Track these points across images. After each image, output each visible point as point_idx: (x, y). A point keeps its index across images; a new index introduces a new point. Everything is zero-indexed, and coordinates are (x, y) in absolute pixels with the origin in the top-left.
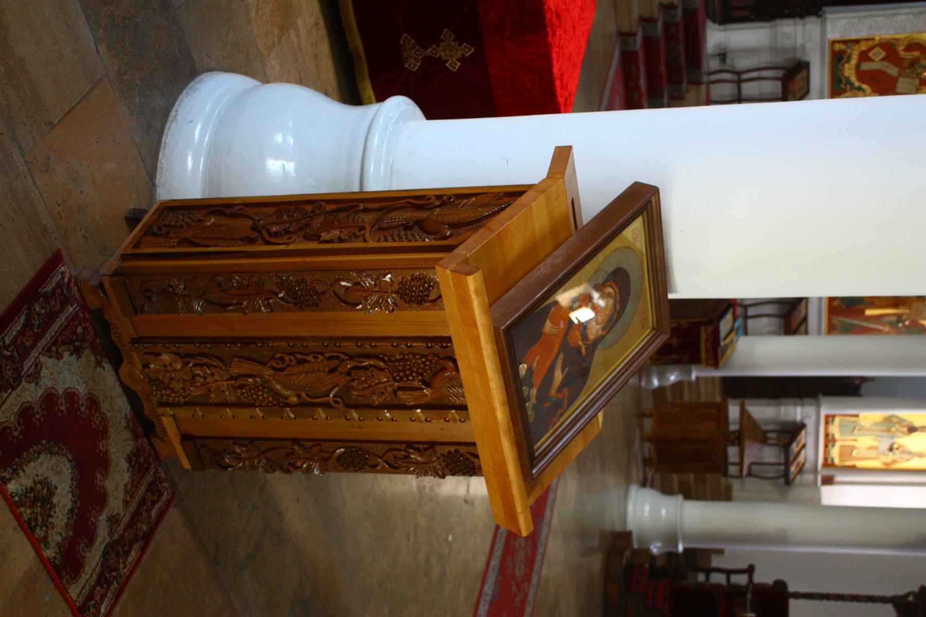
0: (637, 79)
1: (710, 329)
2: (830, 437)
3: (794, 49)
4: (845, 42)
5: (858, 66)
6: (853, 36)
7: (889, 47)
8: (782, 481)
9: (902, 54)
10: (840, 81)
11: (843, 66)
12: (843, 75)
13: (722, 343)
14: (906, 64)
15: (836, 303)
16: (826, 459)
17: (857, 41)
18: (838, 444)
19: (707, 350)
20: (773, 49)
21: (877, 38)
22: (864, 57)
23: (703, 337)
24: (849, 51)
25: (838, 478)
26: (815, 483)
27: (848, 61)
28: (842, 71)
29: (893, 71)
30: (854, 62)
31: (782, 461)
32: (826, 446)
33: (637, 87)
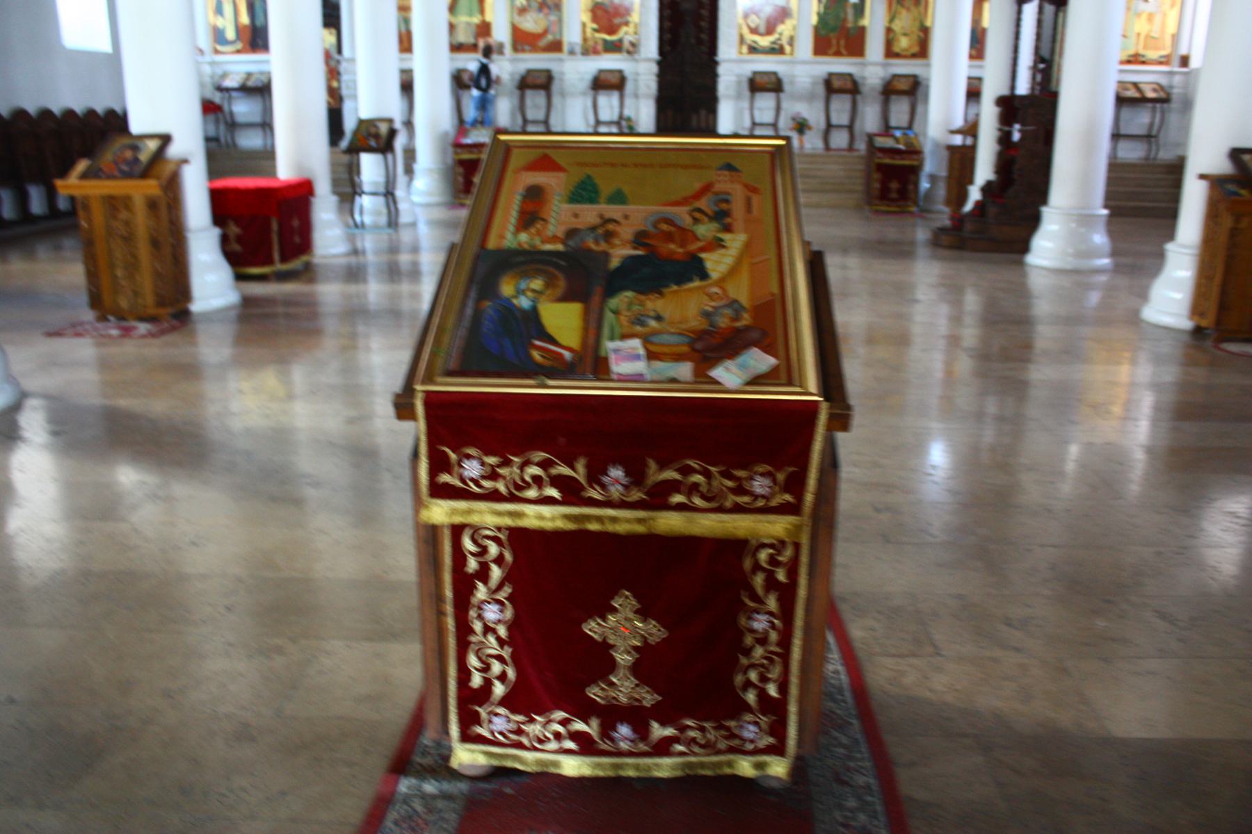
1: (880, 155)
2: (1131, 59)
3: (739, 83)
6: (736, 39)
8: (1165, 105)
11: (761, 47)
13: (901, 147)
15: (974, 53)
16: (1161, 63)
18: (1141, 52)
19: (902, 159)
20: (738, 96)
22: (754, 31)
23: (887, 161)
27: (755, 42)
31: (1150, 105)
32: (1143, 63)
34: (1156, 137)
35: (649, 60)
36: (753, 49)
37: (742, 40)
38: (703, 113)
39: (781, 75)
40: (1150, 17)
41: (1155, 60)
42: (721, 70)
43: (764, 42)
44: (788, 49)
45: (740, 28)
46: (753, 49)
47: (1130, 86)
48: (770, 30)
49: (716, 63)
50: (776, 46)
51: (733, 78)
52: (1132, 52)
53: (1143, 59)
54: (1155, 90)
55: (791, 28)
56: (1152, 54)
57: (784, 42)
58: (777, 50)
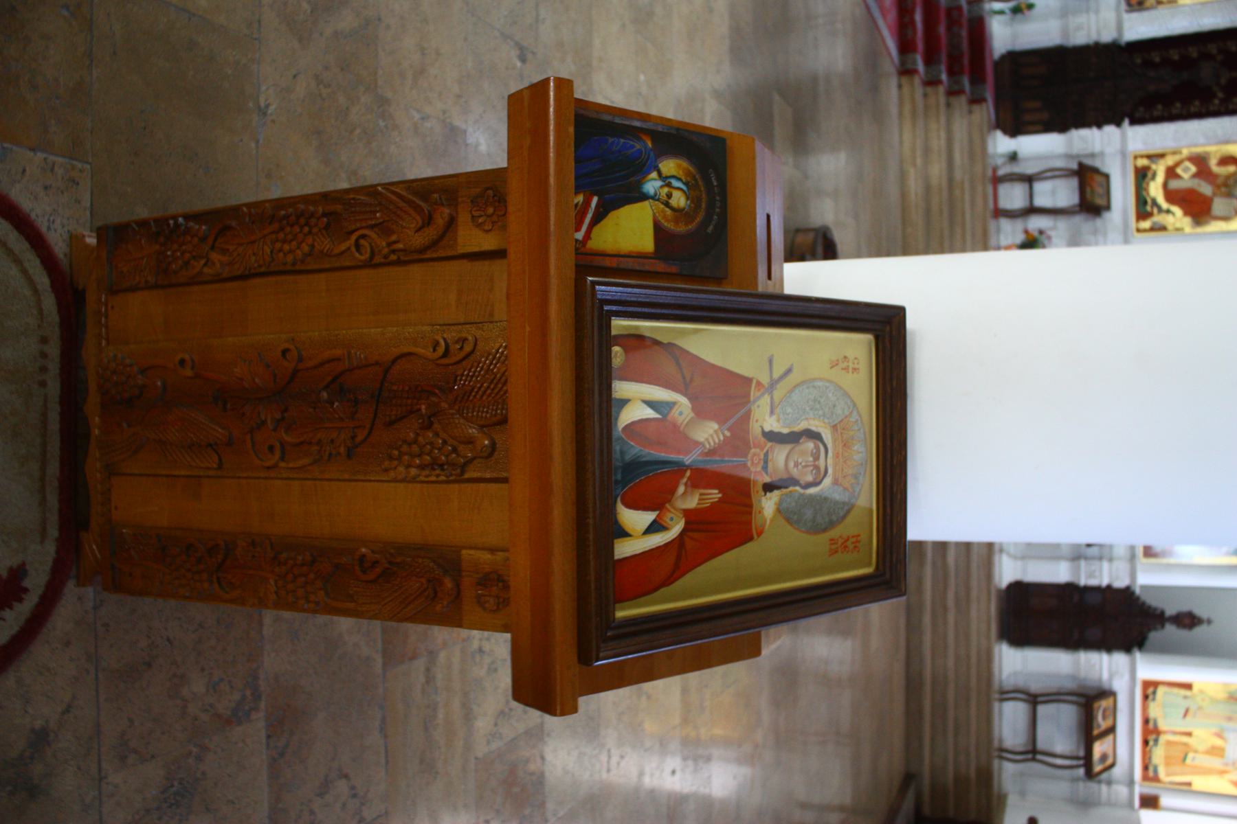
0: (911, 13)
2: (1151, 725)
4: (1149, 157)
5: (1165, 185)
6: (1155, 147)
7: (1200, 161)
8: (1081, 771)
9: (1215, 169)
10: (1145, 203)
11: (1148, 184)
12: (1148, 194)
14: (1220, 181)
16: (1146, 768)
17: (1162, 156)
18: (1163, 739)
21: (1185, 152)
22: (1171, 173)
24: (1154, 167)
25: (1165, 800)
26: (1130, 804)
27: (1154, 177)
28: (1147, 190)
29: (1206, 189)
30: (1160, 178)
31: (1082, 753)
32: (1146, 743)
33: (913, 22)
34: (1034, 759)
35: (1120, 27)
36: (1142, 175)
37: (1155, 157)
38: (1045, 116)
39: (1106, 215)
40: (1216, 751)
41: (1150, 758)
42: (1110, 130)
43: (1155, 190)
44: (1146, 224)
45: (1174, 153)
46: (1142, 175)
47: (1109, 723)
48: (1171, 196)
49: (1118, 124)
50: (1148, 208)
51: (1097, 148)
52: (1162, 725)
53: (1151, 743)
54: (1104, 757)
55: (1178, 225)
56: (1158, 754)
57: (1158, 218)
58: (1144, 208)
